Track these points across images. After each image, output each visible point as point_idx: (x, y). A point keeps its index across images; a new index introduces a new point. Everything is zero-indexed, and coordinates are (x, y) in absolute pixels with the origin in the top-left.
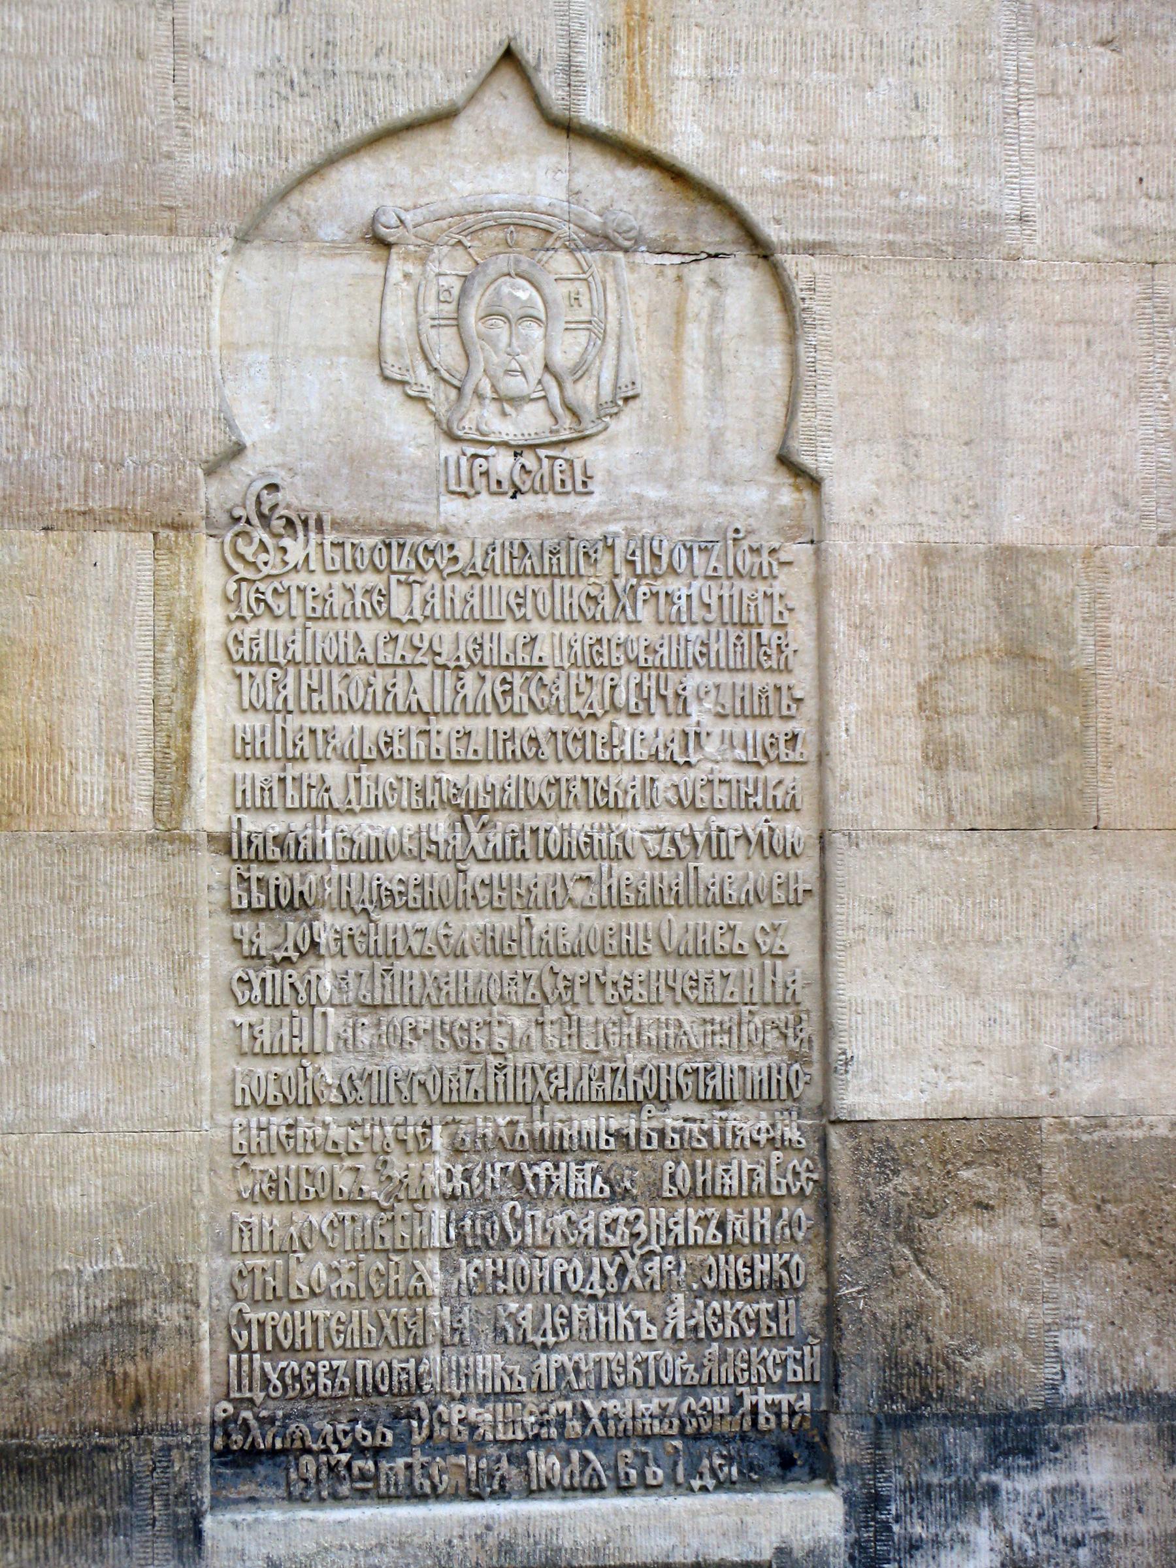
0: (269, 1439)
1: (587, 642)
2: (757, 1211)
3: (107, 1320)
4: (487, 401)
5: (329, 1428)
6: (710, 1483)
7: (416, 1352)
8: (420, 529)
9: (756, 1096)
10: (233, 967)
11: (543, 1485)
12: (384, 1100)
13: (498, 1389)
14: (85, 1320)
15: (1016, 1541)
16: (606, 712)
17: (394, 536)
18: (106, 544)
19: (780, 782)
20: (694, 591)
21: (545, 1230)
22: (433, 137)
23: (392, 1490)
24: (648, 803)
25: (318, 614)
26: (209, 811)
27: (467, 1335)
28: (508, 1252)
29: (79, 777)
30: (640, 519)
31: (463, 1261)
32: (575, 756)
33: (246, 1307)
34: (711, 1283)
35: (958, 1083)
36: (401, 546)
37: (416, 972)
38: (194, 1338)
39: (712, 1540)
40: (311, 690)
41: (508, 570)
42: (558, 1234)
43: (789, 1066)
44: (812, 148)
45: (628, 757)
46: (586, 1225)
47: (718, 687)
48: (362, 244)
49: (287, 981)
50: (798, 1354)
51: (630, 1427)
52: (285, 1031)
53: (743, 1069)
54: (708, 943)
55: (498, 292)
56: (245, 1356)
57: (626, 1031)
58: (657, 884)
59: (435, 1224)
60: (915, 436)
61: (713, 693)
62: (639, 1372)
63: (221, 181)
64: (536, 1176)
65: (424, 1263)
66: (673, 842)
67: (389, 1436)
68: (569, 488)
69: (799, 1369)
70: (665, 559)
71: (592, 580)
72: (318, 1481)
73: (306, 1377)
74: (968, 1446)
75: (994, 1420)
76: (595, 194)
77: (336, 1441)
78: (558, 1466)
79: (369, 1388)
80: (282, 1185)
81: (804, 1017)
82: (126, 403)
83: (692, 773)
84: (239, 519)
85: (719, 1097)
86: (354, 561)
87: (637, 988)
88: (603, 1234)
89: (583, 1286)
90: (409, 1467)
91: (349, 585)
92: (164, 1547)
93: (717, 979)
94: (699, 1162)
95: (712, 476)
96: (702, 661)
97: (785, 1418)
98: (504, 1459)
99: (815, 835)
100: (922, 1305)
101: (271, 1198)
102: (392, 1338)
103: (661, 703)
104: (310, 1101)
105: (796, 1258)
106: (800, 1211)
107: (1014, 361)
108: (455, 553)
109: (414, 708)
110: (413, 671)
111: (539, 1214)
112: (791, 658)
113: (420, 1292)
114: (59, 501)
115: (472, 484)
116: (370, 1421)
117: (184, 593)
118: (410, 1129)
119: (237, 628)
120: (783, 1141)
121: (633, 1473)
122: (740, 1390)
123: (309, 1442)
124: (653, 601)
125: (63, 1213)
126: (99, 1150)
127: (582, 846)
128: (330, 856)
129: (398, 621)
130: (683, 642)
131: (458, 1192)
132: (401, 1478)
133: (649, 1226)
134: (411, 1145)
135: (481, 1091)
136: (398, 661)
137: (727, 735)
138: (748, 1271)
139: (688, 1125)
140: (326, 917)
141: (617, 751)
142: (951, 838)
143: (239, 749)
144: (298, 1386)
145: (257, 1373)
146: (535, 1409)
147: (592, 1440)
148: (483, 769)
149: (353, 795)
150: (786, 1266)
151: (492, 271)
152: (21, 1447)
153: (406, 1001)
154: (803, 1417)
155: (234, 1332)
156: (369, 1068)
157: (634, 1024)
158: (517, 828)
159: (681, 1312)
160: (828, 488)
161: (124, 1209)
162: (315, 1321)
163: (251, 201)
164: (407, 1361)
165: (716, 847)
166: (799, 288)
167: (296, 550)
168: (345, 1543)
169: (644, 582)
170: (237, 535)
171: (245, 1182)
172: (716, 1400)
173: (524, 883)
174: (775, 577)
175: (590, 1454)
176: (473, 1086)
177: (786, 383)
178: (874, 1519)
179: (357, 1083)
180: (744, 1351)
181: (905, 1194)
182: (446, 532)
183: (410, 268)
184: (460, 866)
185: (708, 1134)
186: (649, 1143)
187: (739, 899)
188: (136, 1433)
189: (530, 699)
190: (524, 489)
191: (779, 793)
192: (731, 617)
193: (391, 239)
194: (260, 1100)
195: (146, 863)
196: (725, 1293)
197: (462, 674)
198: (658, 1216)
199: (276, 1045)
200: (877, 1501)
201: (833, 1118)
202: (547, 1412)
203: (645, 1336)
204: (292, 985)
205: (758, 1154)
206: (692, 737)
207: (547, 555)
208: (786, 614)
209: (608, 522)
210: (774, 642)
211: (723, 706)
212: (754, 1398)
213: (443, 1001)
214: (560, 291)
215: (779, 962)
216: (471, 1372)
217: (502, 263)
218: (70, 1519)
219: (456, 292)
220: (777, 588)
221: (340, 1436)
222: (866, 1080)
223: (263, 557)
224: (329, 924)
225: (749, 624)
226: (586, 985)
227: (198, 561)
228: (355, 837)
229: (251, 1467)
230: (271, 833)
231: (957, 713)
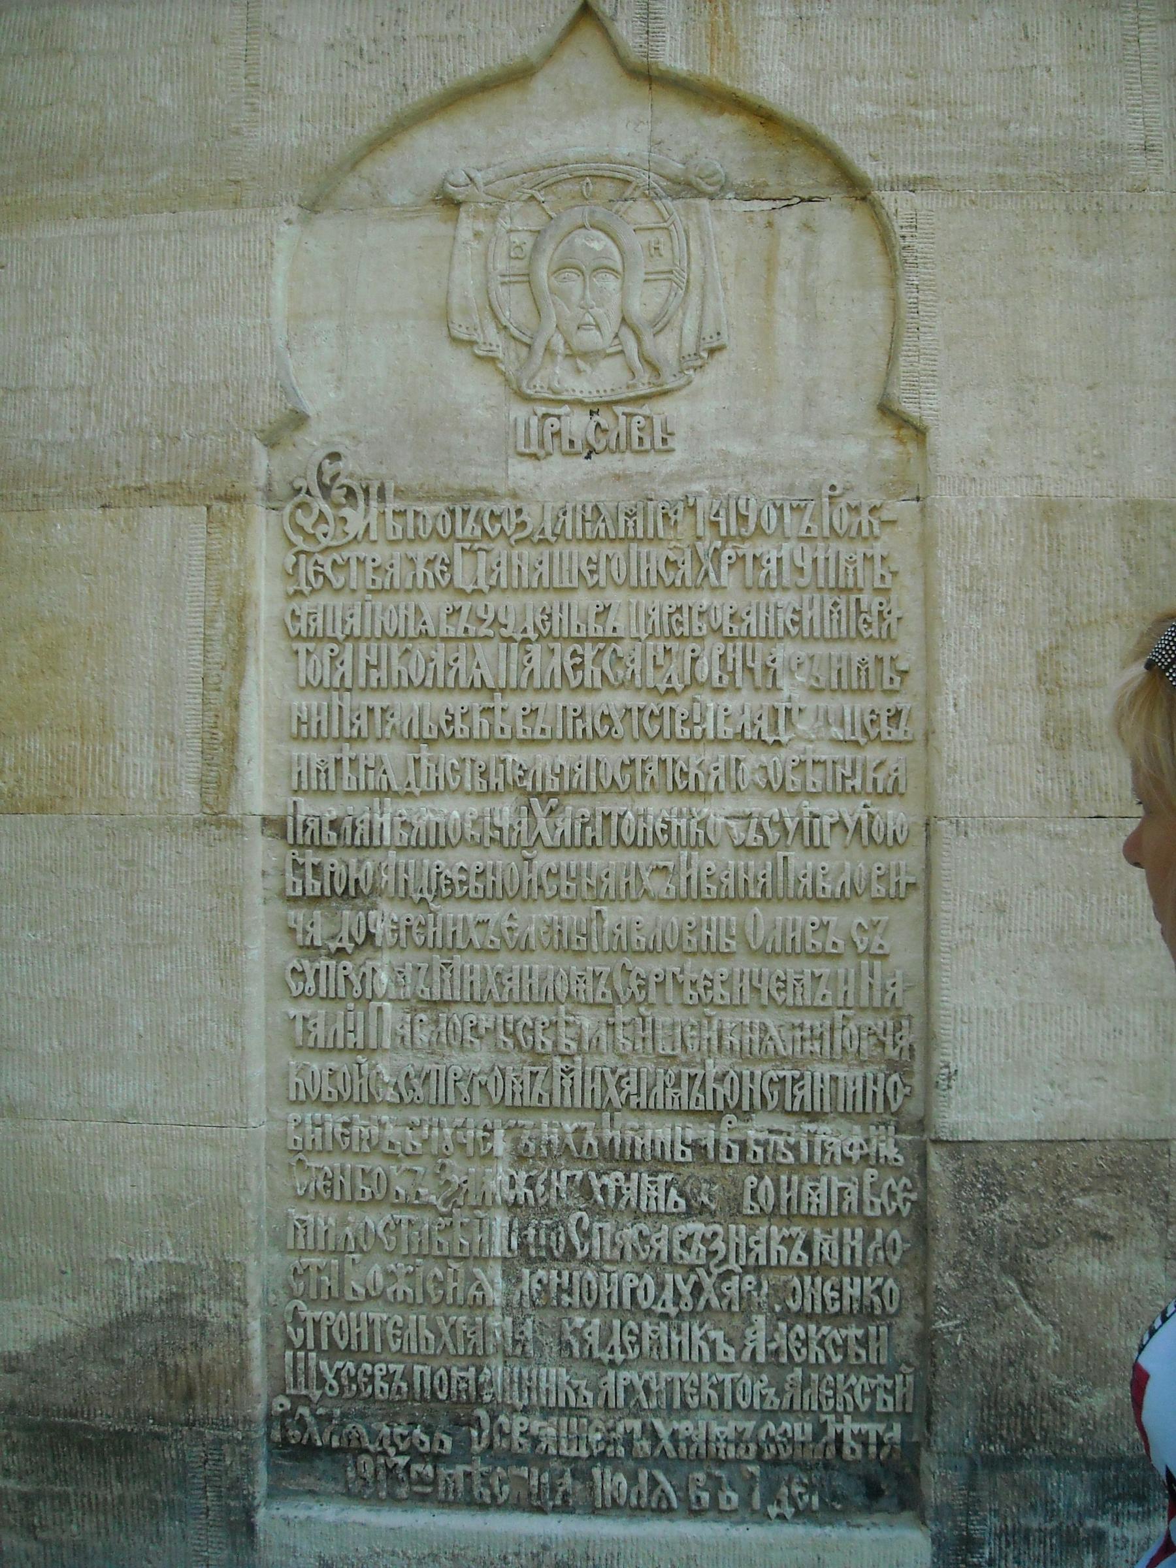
0: (327, 1436)
1: (666, 610)
2: (847, 1232)
4: (560, 358)
5: (387, 1430)
6: (789, 1511)
7: (477, 1362)
8: (488, 494)
9: (849, 1109)
10: (289, 958)
11: (609, 1503)
12: (442, 1100)
13: (562, 1403)
14: (136, 1310)
17: (460, 500)
18: (160, 520)
19: (881, 763)
20: (785, 553)
21: (614, 1244)
22: (509, 98)
23: (451, 1497)
24: (734, 786)
25: (378, 586)
26: (258, 792)
27: (530, 1348)
30: (725, 476)
31: (526, 1272)
32: (652, 734)
33: (302, 1305)
34: (795, 1307)
35: (1076, 1101)
36: (466, 512)
37: (477, 967)
40: (369, 665)
41: (579, 534)
42: (629, 1248)
43: (887, 1077)
44: (911, 83)
45: (711, 735)
46: (658, 1240)
48: (432, 206)
49: (342, 973)
50: (889, 1384)
51: (703, 1451)
52: (340, 1025)
53: (835, 1079)
54: (798, 940)
56: (301, 1354)
57: (706, 1035)
60: (1031, 381)
61: (807, 663)
64: (604, 1188)
65: (485, 1271)
66: (760, 828)
67: (448, 1444)
68: (647, 445)
71: (673, 544)
72: (376, 1481)
73: (362, 1379)
74: (1071, 1490)
75: (1103, 1464)
76: (677, 143)
77: (393, 1444)
78: (625, 1485)
79: (428, 1395)
81: (905, 1023)
83: (783, 753)
85: (808, 1108)
86: (416, 529)
87: (719, 989)
88: (677, 1250)
89: (655, 1302)
90: (468, 1475)
91: (411, 555)
93: (807, 981)
94: (784, 1178)
95: (806, 429)
96: (794, 631)
97: (873, 1449)
98: (568, 1474)
99: (921, 822)
100: (1027, 1342)
101: (326, 1196)
102: (450, 1346)
103: (748, 675)
104: (365, 1099)
105: (890, 1282)
106: (895, 1234)
107: (1142, 298)
109: (478, 684)
110: (478, 645)
111: (608, 1227)
112: (894, 626)
113: (479, 1301)
115: (542, 444)
116: (430, 1426)
117: (235, 566)
118: (471, 1133)
119: (294, 605)
120: (878, 1158)
121: (705, 1496)
122: (823, 1418)
123: (366, 1444)
124: (740, 564)
126: (147, 1142)
127: (659, 833)
128: (387, 843)
129: (462, 591)
130: (772, 610)
131: (521, 1200)
132: (461, 1486)
133: (727, 1243)
134: (470, 1149)
135: (546, 1095)
136: (461, 633)
137: (821, 712)
138: (836, 1294)
139: (773, 1138)
140: (384, 905)
141: (698, 730)
142: (1074, 827)
143: (295, 730)
144: (354, 1387)
146: (601, 1426)
148: (553, 748)
150: (878, 1290)
153: (467, 997)
155: (290, 1329)
156: (428, 1067)
157: (715, 1027)
158: (588, 813)
159: (762, 1335)
160: (931, 438)
162: (371, 1324)
165: (807, 835)
166: (898, 225)
167: (356, 519)
169: (730, 545)
170: (299, 506)
171: (300, 1180)
173: (594, 873)
175: (660, 1476)
176: (538, 1089)
177: (889, 329)
178: (964, 1561)
179: (416, 1082)
182: (515, 496)
183: (480, 226)
184: (526, 853)
185: (795, 1148)
186: (729, 1156)
187: (833, 893)
188: (190, 1424)
190: (598, 448)
191: (880, 776)
193: (460, 197)
194: (314, 1095)
196: (811, 1317)
197: (529, 647)
198: (737, 1234)
199: (331, 1039)
201: (933, 1137)
202: (614, 1429)
206: (782, 713)
207: (622, 518)
208: (888, 577)
209: (691, 481)
210: (875, 608)
211: (817, 679)
212: (839, 1427)
213: (506, 998)
214: (638, 242)
215: (877, 963)
216: (533, 1384)
217: (578, 215)
218: (128, 1500)
219: (528, 248)
220: (878, 549)
221: (398, 1440)
222: (972, 1096)
223: (323, 528)
224: (386, 916)
225: (847, 590)
228: (414, 822)
230: (328, 817)
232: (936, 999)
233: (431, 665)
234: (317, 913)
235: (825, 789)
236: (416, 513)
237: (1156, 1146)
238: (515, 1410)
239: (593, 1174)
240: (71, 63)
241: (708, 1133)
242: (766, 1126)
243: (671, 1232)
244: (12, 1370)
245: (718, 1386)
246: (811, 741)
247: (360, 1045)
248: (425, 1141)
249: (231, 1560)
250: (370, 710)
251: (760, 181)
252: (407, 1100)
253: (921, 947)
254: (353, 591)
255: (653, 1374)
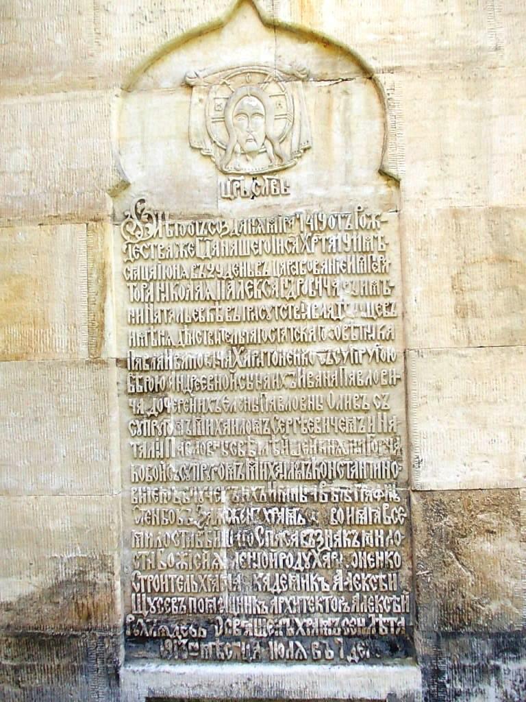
0: (151, 632)
1: (288, 264)
2: (377, 532)
3: (74, 580)
4: (239, 155)
5: (177, 628)
6: (356, 659)
7: (216, 594)
8: (209, 216)
9: (375, 477)
11: (277, 658)
12: (198, 479)
13: (255, 612)
14: (64, 579)
15: (509, 693)
16: (298, 297)
17: (198, 220)
18: (65, 230)
19: (384, 327)
21: (275, 540)
22: (212, 38)
23: (207, 657)
25: (163, 257)
26: (114, 348)
27: (239, 587)
28: (257, 549)
29: (56, 335)
31: (237, 553)
32: (284, 318)
33: (140, 573)
35: (477, 472)
36: (200, 224)
37: (212, 420)
38: (113, 589)
39: (357, 689)
41: (250, 232)
42: (281, 541)
43: (391, 463)
45: (309, 317)
47: (352, 283)
50: (398, 599)
51: (317, 632)
53: (369, 464)
55: (242, 104)
56: (139, 595)
57: (311, 446)
58: (325, 377)
59: (223, 535)
62: (321, 606)
63: (115, 64)
64: (270, 515)
66: (332, 357)
69: (399, 606)
70: (325, 223)
71: (290, 235)
72: (173, 651)
74: (484, 648)
75: (498, 635)
77: (180, 634)
79: (195, 611)
80: (153, 519)
81: (398, 439)
82: (73, 166)
84: (127, 216)
85: (357, 477)
87: (316, 426)
88: (302, 542)
89: (294, 565)
90: (214, 647)
92: (103, 681)
93: (355, 422)
94: (348, 509)
95: (346, 183)
96: (344, 271)
97: (392, 629)
98: (258, 645)
102: (205, 588)
104: (165, 480)
105: (397, 554)
106: (398, 532)
107: (496, 116)
108: (225, 225)
109: (208, 298)
110: (207, 281)
111: (271, 532)
112: (387, 267)
113: (217, 567)
114: (46, 212)
115: (232, 193)
117: (100, 250)
118: (211, 493)
119: (127, 266)
120: (389, 498)
121: (319, 653)
122: (370, 615)
123: (168, 634)
124: (320, 243)
125: (54, 532)
126: (68, 503)
128: (171, 368)
129: (200, 258)
131: (234, 522)
132: (211, 652)
134: (211, 500)
135: (243, 476)
136: (200, 277)
138: (373, 560)
139: (342, 491)
142: (471, 352)
143: (129, 320)
145: (144, 603)
146: (272, 622)
147: (299, 637)
149: (181, 340)
150: (391, 557)
151: (239, 94)
152: (39, 634)
154: (401, 629)
156: (191, 464)
158: (257, 352)
159: (341, 579)
161: (80, 530)
162: (169, 580)
163: (128, 72)
164: (212, 598)
165: (352, 358)
167: (152, 228)
168: (183, 683)
170: (127, 223)
171: (137, 516)
172: (359, 620)
174: (379, 229)
175: (298, 643)
176: (239, 473)
178: (437, 681)
179: (186, 472)
180: (372, 597)
181: (451, 526)
182: (221, 216)
183: (202, 96)
185: (352, 495)
186: (324, 499)
189: (262, 292)
190: (257, 194)
191: (383, 333)
192: (357, 249)
193: (192, 83)
194: (142, 479)
195: (86, 373)
196: (362, 570)
200: (438, 673)
202: (278, 623)
203: (323, 589)
204: (155, 427)
205: (377, 504)
206: (340, 306)
207: (268, 224)
208: (384, 246)
209: (296, 208)
212: (377, 619)
213: (224, 433)
214: (271, 102)
215: (385, 413)
216: (242, 604)
218: (62, 667)
220: (379, 234)
221: (182, 632)
222: (429, 471)
223: (138, 232)
224: (172, 399)
226: (291, 425)
227: (106, 235)
229: (144, 644)
231: (472, 290)
232: (412, 428)
233: (188, 291)
234: (142, 400)
235: (359, 339)
236: (179, 225)
237: (513, 491)
238: (234, 616)
239: (264, 509)
240: (15, 24)
241: (313, 489)
242: (339, 485)
243: (299, 533)
244: (8, 610)
245: (323, 602)
246: (352, 318)
247: (162, 457)
248: (192, 497)
249: (108, 692)
250: (162, 311)
251: (325, 72)
252: (183, 479)
253: (404, 406)
254: (153, 260)
255: (294, 597)
